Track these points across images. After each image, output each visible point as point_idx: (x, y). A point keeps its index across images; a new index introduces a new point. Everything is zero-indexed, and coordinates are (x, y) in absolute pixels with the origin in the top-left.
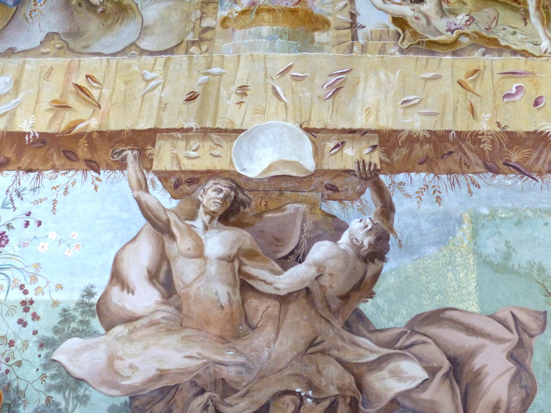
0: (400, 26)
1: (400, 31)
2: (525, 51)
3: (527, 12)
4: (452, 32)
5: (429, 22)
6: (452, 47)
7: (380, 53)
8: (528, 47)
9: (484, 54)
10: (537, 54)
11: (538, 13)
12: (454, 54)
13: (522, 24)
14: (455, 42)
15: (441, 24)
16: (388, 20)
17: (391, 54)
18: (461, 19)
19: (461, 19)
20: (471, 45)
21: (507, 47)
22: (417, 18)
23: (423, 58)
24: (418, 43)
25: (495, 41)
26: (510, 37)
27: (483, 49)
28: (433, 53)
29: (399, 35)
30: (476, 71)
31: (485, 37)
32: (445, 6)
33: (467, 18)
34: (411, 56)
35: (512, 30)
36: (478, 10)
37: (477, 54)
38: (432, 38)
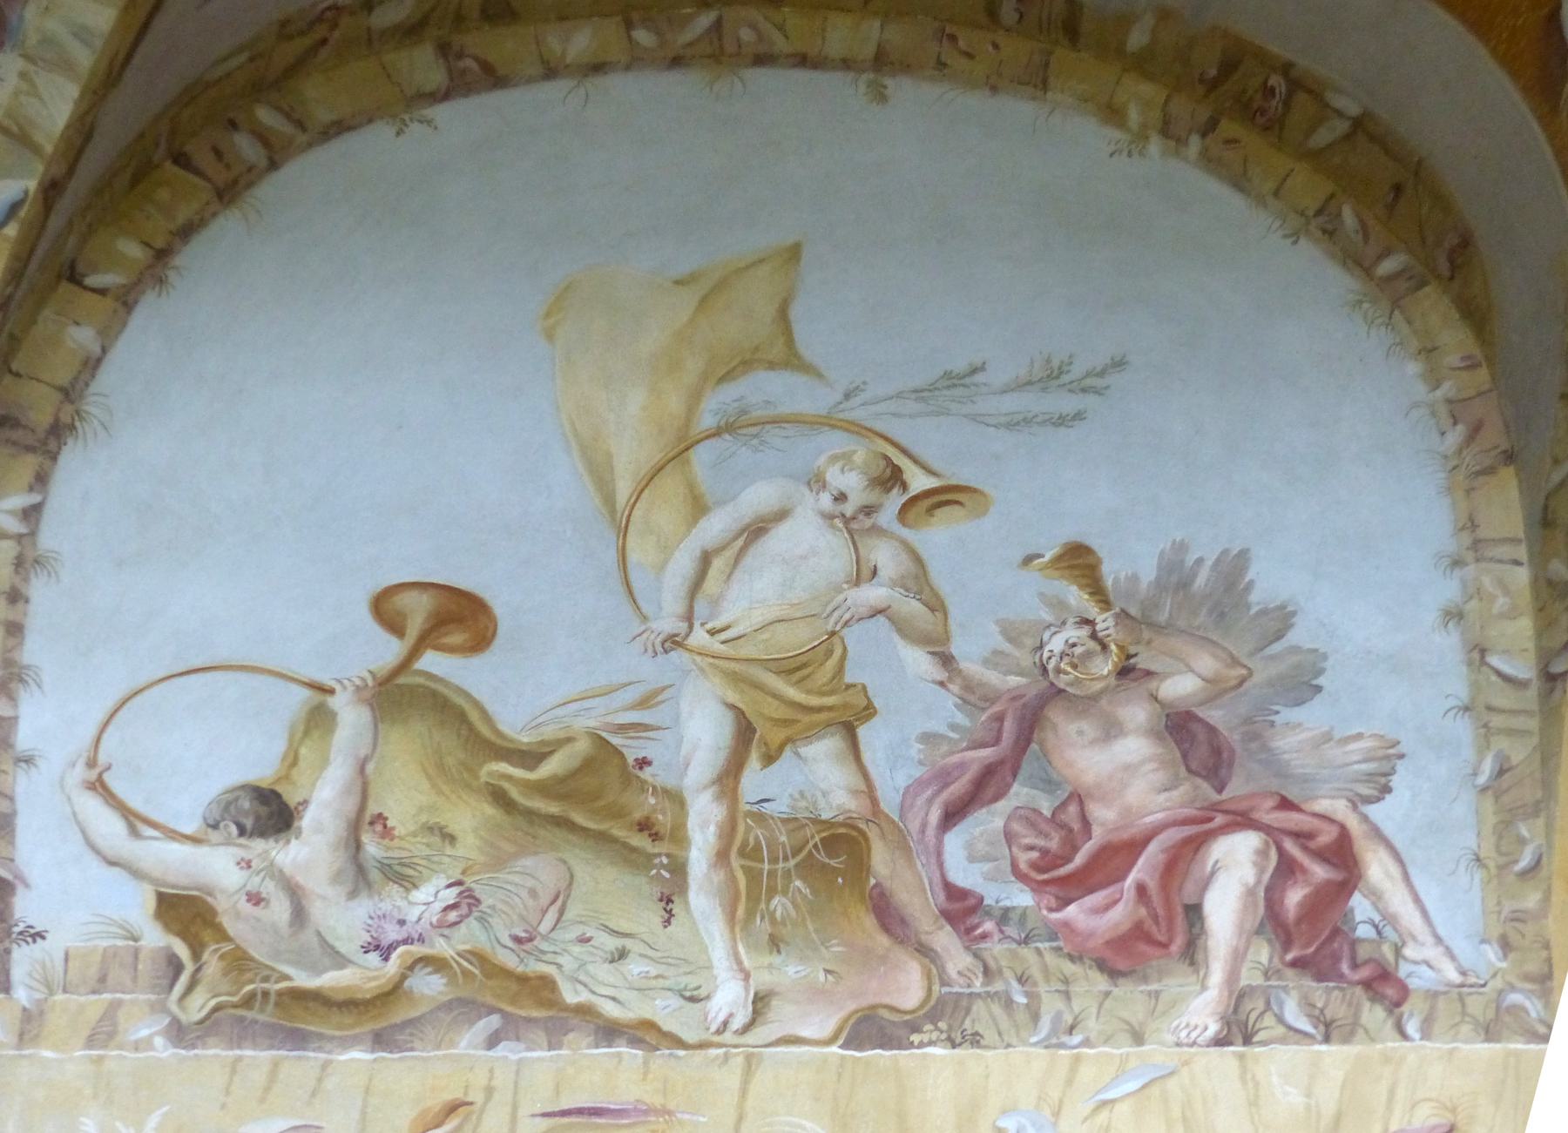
0: (183, 935)
1: (182, 950)
2: (650, 1025)
3: (679, 870)
4: (386, 952)
5: (299, 915)
6: (376, 1015)
7: (91, 1042)
8: (664, 1011)
9: (493, 1041)
10: (690, 1036)
11: (719, 877)
12: (381, 1041)
13: (655, 916)
14: (393, 993)
15: (344, 919)
16: (137, 907)
17: (137, 1047)
18: (428, 898)
19: (428, 898)
20: (448, 1006)
21: (584, 1011)
22: (256, 899)
23: (257, 1057)
24: (248, 1001)
25: (541, 989)
26: (603, 971)
27: (494, 1021)
28: (298, 1039)
29: (176, 967)
30: (453, 1108)
31: (507, 974)
32: (372, 848)
33: (450, 895)
34: (215, 1053)
35: (612, 943)
36: (498, 862)
37: (469, 1040)
38: (303, 980)
